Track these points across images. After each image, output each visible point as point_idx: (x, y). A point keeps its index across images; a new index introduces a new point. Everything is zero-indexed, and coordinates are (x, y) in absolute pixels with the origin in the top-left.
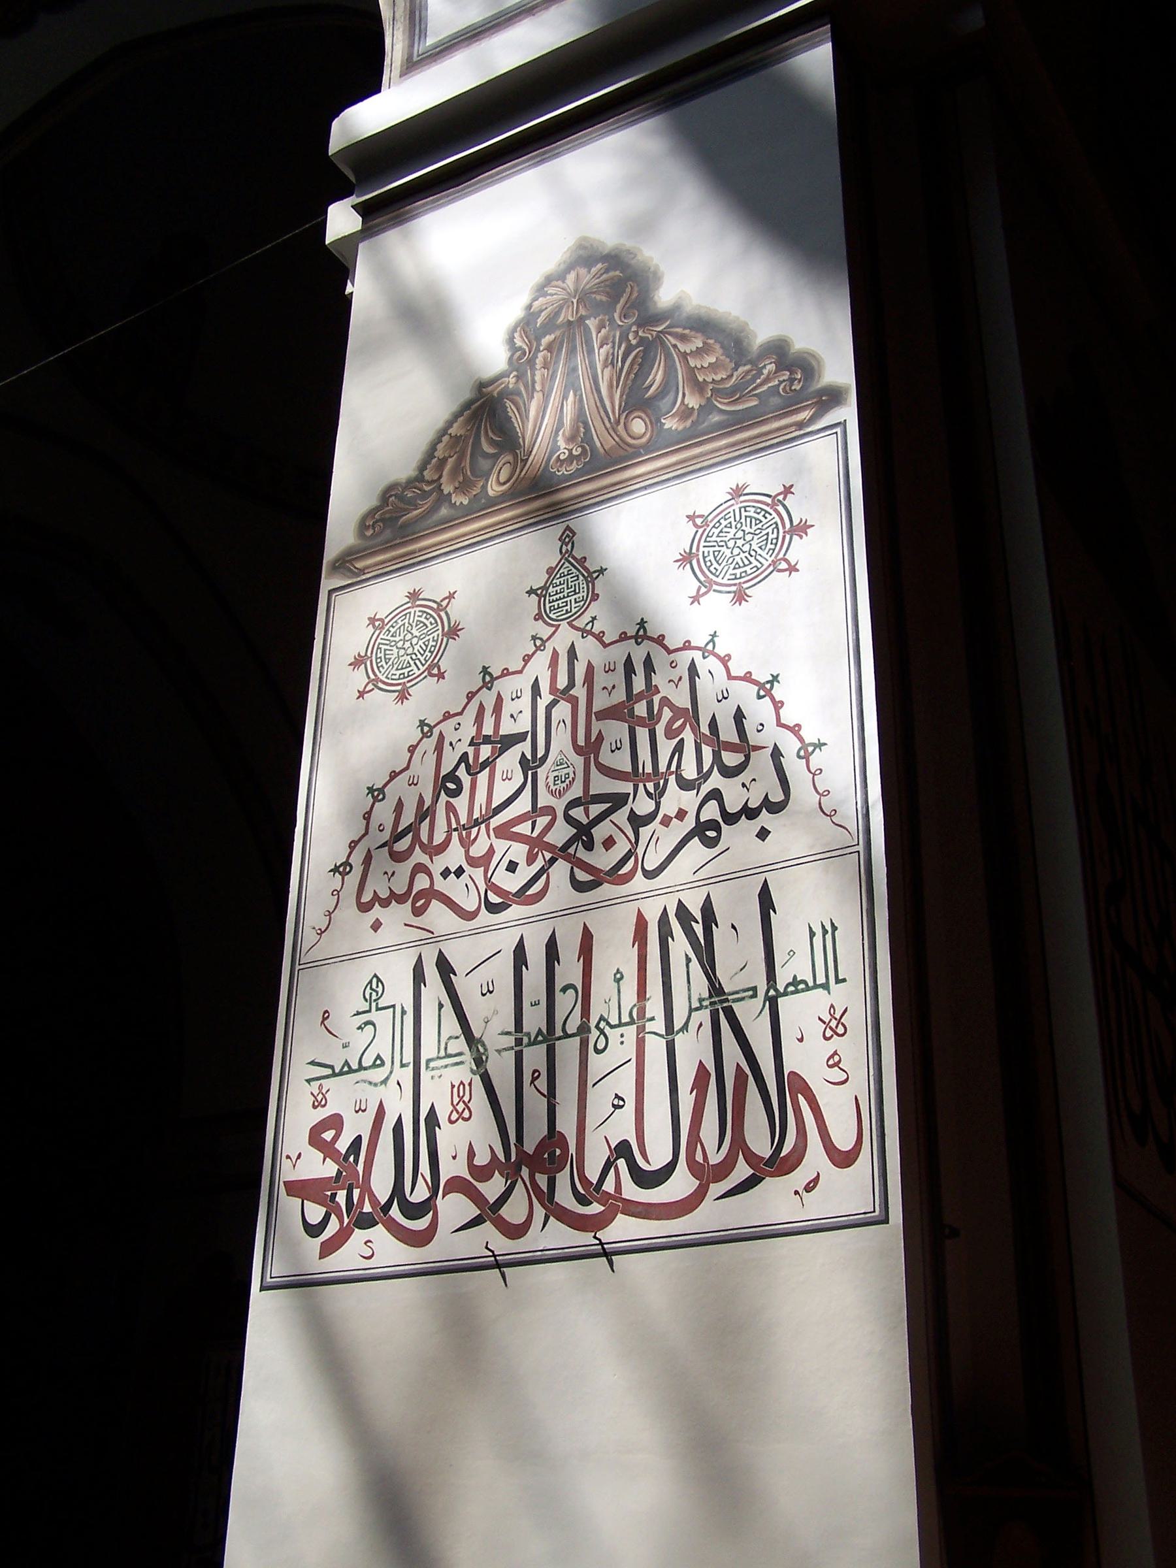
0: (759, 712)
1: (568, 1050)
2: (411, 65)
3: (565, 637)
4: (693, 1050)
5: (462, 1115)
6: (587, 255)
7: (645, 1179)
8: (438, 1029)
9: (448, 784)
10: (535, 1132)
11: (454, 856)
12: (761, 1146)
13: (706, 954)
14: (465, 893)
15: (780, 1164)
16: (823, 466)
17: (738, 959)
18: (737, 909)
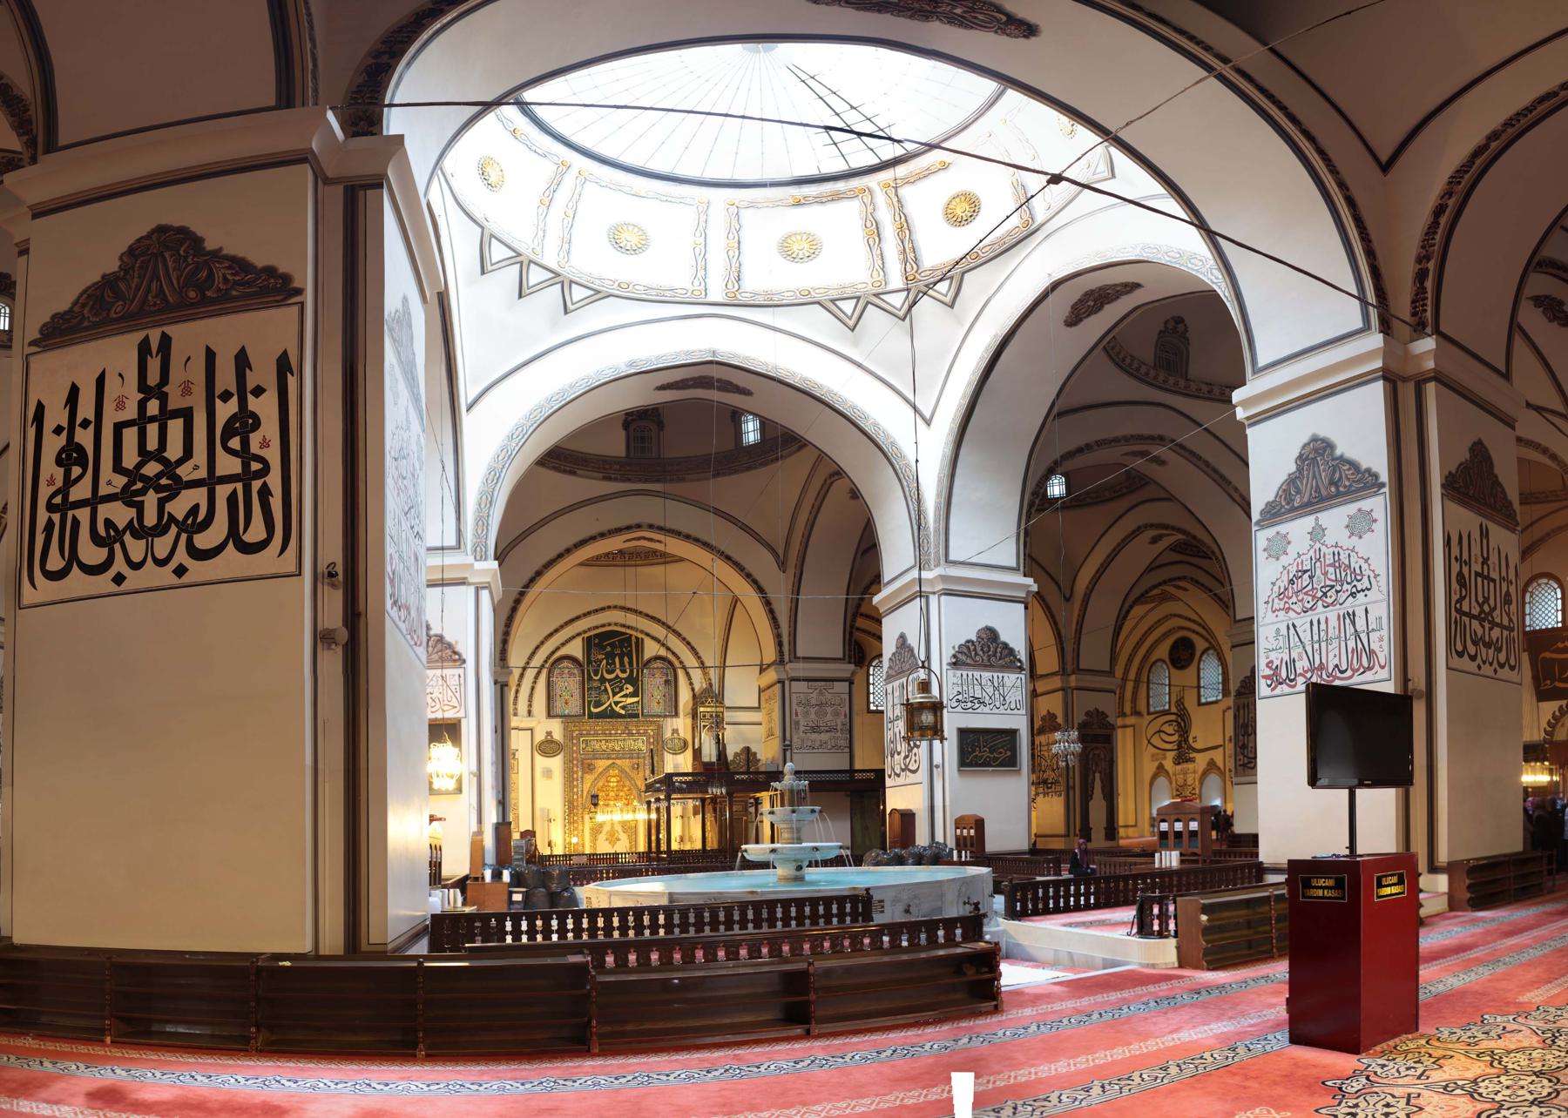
0: (1365, 566)
1: (1323, 645)
2: (1257, 371)
3: (1318, 546)
4: (1351, 644)
5: (1301, 659)
6: (1314, 439)
7: (1342, 672)
8: (1294, 639)
9: (1291, 582)
10: (1317, 662)
11: (1294, 599)
12: (1365, 664)
13: (1353, 623)
14: (1298, 608)
15: (1369, 669)
16: (1378, 506)
17: (1360, 623)
18: (1360, 613)
